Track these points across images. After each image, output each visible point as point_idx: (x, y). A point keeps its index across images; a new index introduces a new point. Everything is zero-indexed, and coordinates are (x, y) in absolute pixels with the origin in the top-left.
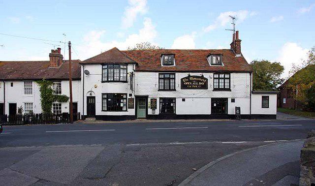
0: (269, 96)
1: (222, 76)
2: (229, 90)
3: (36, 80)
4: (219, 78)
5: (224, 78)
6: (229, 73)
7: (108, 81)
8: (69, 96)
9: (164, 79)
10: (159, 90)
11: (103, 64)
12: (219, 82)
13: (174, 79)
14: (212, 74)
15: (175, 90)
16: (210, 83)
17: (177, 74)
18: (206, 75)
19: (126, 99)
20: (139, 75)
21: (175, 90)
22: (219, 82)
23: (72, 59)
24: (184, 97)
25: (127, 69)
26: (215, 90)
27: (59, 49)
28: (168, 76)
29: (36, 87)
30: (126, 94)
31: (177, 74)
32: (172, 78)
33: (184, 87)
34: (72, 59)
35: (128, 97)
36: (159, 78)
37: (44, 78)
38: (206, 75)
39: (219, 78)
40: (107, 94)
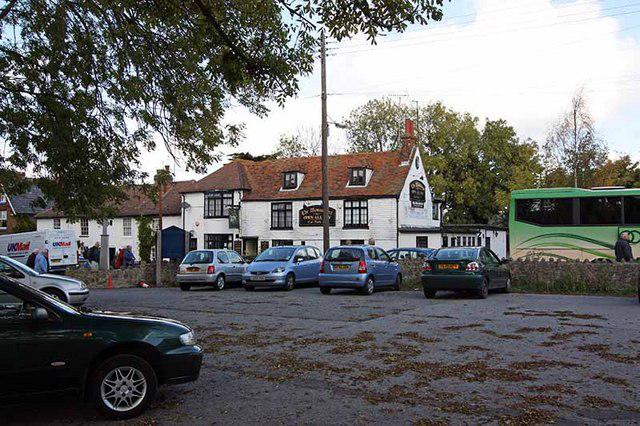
0: (427, 238)
1: (356, 204)
2: (366, 227)
3: (135, 217)
4: (352, 208)
5: (360, 208)
6: (365, 198)
7: (209, 217)
8: (339, 251)
9: (278, 211)
10: (272, 228)
11: (205, 192)
12: (360, 214)
13: (367, 208)
14: (341, 202)
15: (291, 228)
16: (339, 216)
17: (294, 203)
18: (332, 204)
19: (232, 241)
20: (246, 208)
21: (291, 228)
22: (360, 214)
23: (330, 152)
24: (303, 238)
25: (232, 198)
26: (346, 227)
27: (167, 167)
28: (282, 207)
29: (135, 225)
30: (232, 235)
31: (294, 203)
32: (364, 208)
33: (303, 223)
34: (330, 152)
35: (235, 239)
36: (273, 211)
37: (142, 214)
38: (332, 204)
39: (352, 208)
40: (209, 235)
